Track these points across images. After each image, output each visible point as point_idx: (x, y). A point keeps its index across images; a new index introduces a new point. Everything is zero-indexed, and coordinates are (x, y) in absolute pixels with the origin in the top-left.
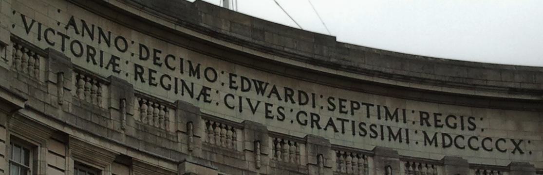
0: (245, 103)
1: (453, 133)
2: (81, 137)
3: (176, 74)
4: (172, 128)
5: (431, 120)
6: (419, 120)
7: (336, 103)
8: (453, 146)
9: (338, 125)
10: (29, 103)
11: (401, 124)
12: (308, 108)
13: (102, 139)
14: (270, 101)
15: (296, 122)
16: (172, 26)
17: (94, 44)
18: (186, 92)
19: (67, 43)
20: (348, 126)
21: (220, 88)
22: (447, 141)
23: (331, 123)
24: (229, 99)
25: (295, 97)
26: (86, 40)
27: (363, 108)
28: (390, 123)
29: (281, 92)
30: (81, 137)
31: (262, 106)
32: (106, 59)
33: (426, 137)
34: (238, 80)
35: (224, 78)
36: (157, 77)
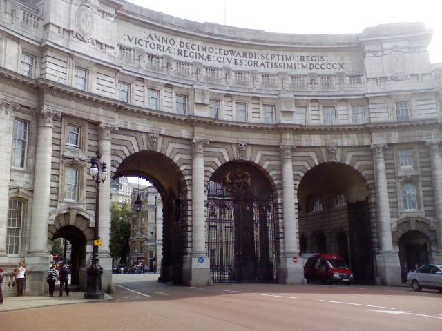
0: (226, 60)
1: (314, 63)
2: (149, 79)
3: (196, 51)
4: (190, 72)
5: (305, 59)
6: (299, 60)
7: (265, 56)
9: (265, 64)
10: (123, 68)
11: (292, 62)
12: (253, 59)
13: (158, 79)
16: (192, 33)
17: (160, 43)
18: (201, 59)
19: (148, 44)
20: (270, 65)
21: (215, 55)
22: (312, 66)
23: (262, 64)
24: (219, 59)
25: (247, 56)
26: (157, 42)
27: (276, 57)
28: (287, 61)
29: (241, 54)
30: (149, 79)
31: (233, 61)
32: (165, 49)
33: (303, 66)
34: (223, 51)
35: (217, 51)
36: (188, 53)
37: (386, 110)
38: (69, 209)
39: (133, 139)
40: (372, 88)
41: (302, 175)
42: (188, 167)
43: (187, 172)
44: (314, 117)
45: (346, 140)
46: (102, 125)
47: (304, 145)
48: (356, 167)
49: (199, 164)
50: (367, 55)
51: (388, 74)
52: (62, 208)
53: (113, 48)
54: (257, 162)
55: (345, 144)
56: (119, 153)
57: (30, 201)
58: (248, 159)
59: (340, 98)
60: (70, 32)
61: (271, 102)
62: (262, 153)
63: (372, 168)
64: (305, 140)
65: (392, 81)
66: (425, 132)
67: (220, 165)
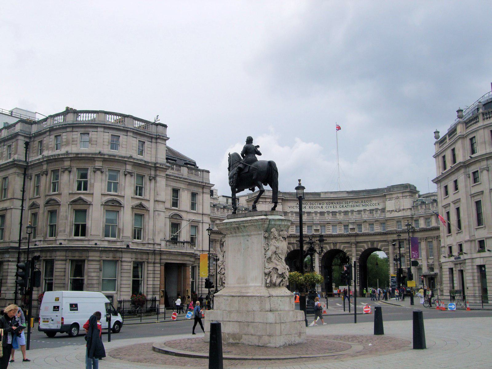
0: (329, 207)
1: (367, 203)
5: (363, 202)
8: (367, 206)
9: (347, 206)
11: (359, 204)
12: (341, 205)
14: (334, 205)
15: (339, 208)
22: (366, 205)
23: (346, 206)
24: (327, 207)
31: (333, 207)
32: (304, 207)
35: (326, 204)
36: (313, 207)
37: (393, 225)
50: (388, 200)
51: (394, 209)
55: (377, 240)
59: (374, 220)
61: (347, 224)
62: (344, 245)
65: (396, 213)
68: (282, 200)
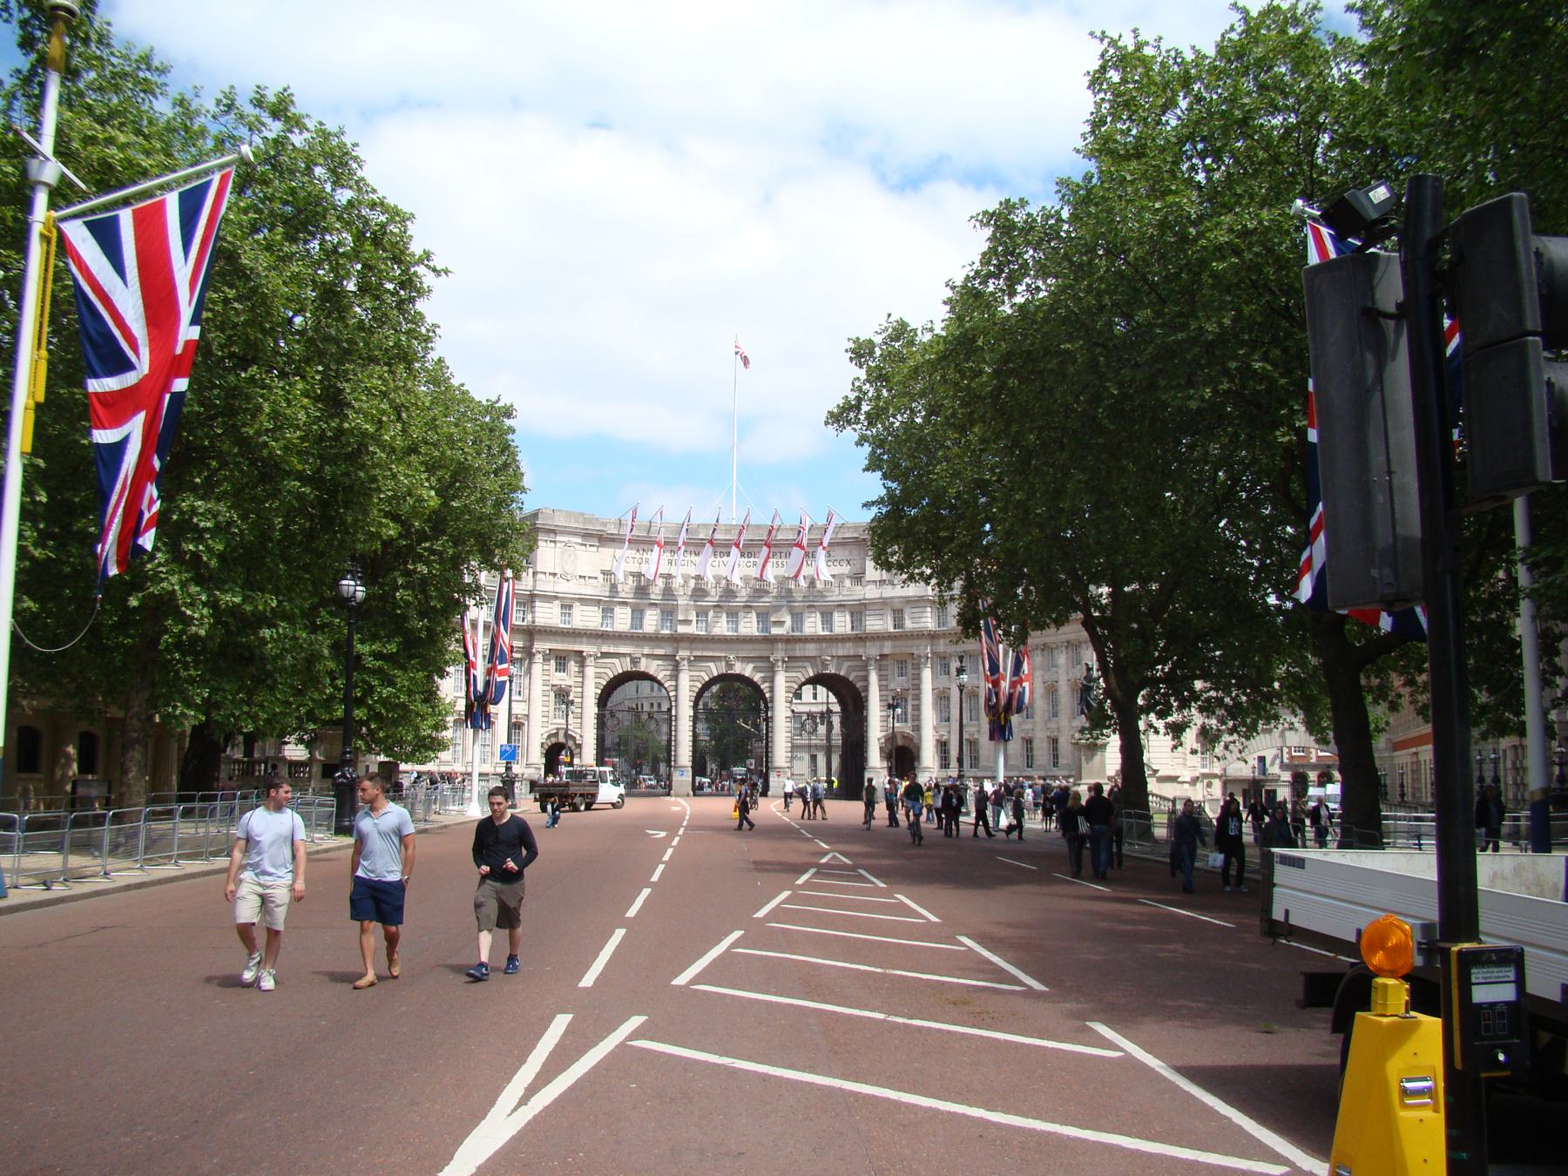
12: (752, 559)
38: (558, 729)
39: (616, 661)
40: (871, 592)
41: (796, 687)
42: (674, 683)
43: (672, 688)
44: (809, 625)
45: (842, 650)
46: (584, 654)
47: (798, 654)
48: (851, 679)
49: (684, 678)
52: (552, 728)
53: (596, 578)
54: (747, 675)
55: (841, 653)
56: (604, 676)
57: (526, 723)
58: (738, 672)
60: (555, 575)
63: (866, 679)
64: (799, 650)
66: (917, 642)
67: (707, 679)
68: (599, 541)
